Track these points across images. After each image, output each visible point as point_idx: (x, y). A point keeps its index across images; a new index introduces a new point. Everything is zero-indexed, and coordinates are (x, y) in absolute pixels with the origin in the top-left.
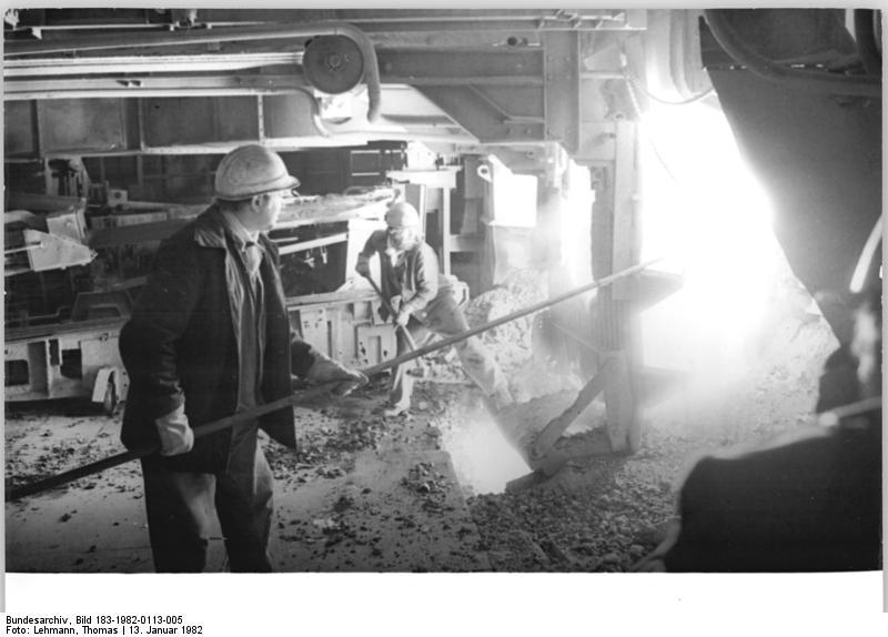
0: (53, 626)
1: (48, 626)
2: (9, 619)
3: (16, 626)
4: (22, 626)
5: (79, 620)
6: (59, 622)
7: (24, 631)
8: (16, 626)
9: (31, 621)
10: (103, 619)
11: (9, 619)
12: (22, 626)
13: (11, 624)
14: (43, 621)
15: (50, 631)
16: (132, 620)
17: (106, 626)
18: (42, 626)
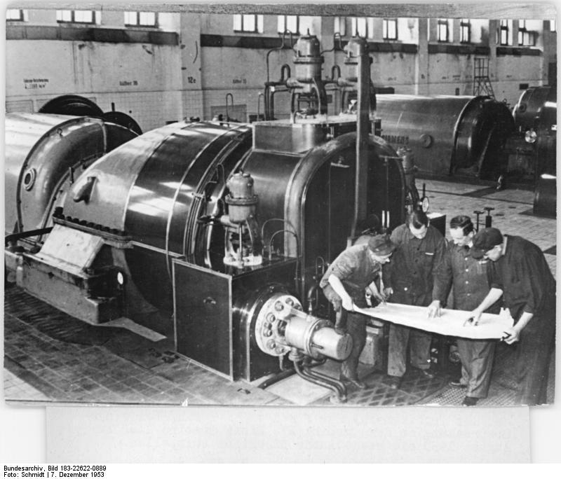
0: (36, 472)
1: (31, 472)
2: (5, 468)
3: (10, 472)
4: (13, 472)
5: (50, 468)
6: (38, 469)
7: (15, 475)
8: (10, 472)
9: (20, 469)
10: (65, 467)
11: (5, 468)
12: (13, 472)
13: (7, 471)
14: (27, 469)
15: (32, 475)
16: (77, 468)
17: (66, 472)
18: (27, 472)
